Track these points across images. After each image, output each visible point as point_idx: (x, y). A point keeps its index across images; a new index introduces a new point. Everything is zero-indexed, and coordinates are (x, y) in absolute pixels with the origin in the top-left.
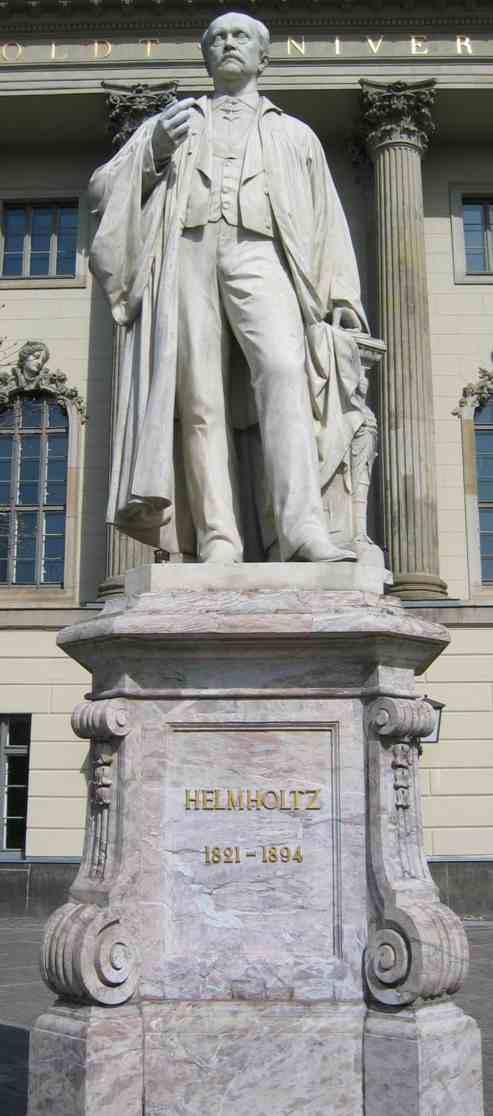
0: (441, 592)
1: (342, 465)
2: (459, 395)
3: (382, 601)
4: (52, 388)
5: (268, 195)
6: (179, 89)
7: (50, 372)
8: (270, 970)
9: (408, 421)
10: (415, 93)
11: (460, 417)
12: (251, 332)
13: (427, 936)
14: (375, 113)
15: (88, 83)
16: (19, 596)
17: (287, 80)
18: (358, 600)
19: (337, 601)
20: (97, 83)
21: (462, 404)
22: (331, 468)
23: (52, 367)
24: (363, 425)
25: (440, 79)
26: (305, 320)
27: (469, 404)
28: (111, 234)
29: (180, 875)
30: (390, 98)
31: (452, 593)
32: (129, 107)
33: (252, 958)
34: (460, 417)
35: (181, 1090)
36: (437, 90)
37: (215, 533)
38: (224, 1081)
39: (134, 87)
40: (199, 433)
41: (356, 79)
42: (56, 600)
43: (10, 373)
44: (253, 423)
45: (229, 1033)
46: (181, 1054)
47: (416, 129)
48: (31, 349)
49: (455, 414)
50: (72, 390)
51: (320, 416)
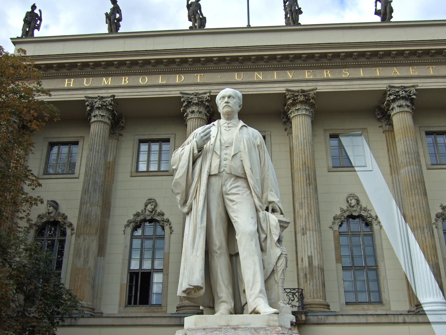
0: (327, 308)
1: (273, 271)
2: (332, 220)
3: (290, 331)
4: (158, 218)
5: (242, 161)
6: (211, 94)
7: (157, 212)
10: (308, 94)
12: (236, 217)
14: (291, 103)
15: (174, 92)
16: (142, 311)
17: (255, 90)
18: (279, 331)
19: (271, 332)
20: (178, 92)
21: (334, 223)
22: (269, 273)
23: (158, 210)
24: (281, 254)
25: (318, 88)
26: (257, 210)
27: (336, 223)
28: (180, 178)
30: (297, 96)
31: (332, 308)
32: (191, 101)
34: (333, 229)
36: (316, 92)
37: (222, 300)
39: (193, 93)
40: (215, 258)
41: (284, 89)
42: (158, 312)
43: (140, 212)
44: (237, 252)
47: (309, 108)
48: (151, 201)
49: (331, 228)
50: (166, 219)
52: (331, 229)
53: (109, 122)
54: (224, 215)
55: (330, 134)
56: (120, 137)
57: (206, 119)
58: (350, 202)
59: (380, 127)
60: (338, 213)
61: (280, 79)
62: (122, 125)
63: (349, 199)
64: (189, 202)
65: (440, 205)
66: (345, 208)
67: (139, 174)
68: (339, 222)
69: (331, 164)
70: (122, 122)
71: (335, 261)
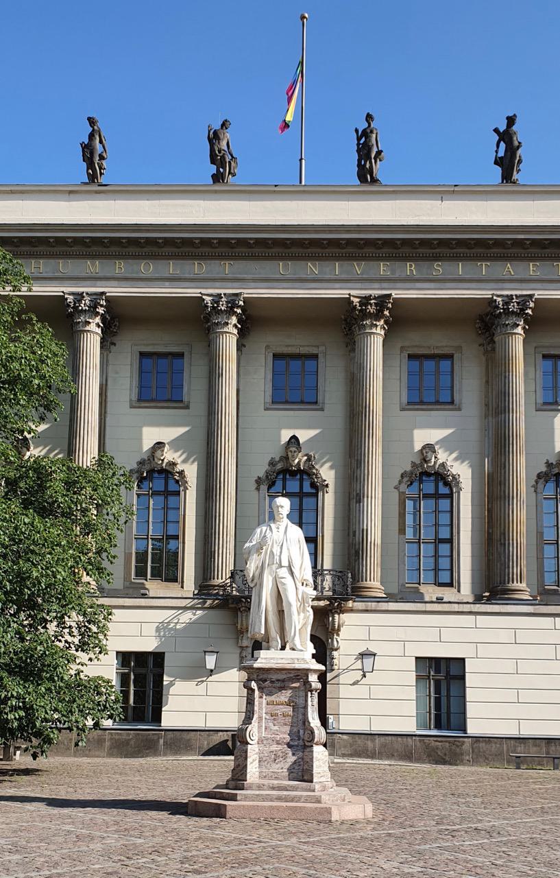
8: (284, 738)
9: (366, 499)
11: (399, 490)
13: (316, 732)
21: (400, 482)
29: (266, 718)
33: (281, 736)
35: (266, 762)
38: (275, 760)
45: (276, 751)
46: (266, 755)
51: (299, 614)
52: (396, 490)
53: (100, 332)
54: (276, 589)
55: (409, 354)
56: (112, 347)
57: (236, 333)
58: (425, 454)
59: (480, 345)
60: (408, 468)
61: (344, 276)
62: (115, 330)
63: (424, 451)
64: (255, 581)
65: (546, 461)
66: (418, 462)
67: (143, 405)
68: (407, 481)
69: (405, 400)
70: (115, 326)
71: (398, 531)
